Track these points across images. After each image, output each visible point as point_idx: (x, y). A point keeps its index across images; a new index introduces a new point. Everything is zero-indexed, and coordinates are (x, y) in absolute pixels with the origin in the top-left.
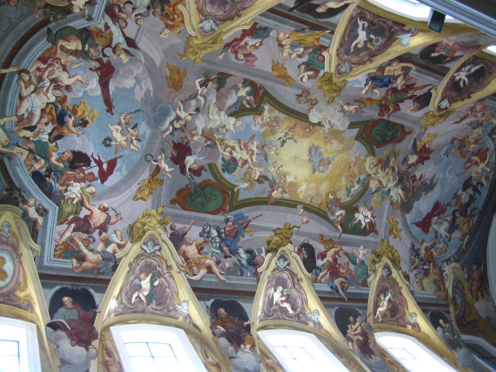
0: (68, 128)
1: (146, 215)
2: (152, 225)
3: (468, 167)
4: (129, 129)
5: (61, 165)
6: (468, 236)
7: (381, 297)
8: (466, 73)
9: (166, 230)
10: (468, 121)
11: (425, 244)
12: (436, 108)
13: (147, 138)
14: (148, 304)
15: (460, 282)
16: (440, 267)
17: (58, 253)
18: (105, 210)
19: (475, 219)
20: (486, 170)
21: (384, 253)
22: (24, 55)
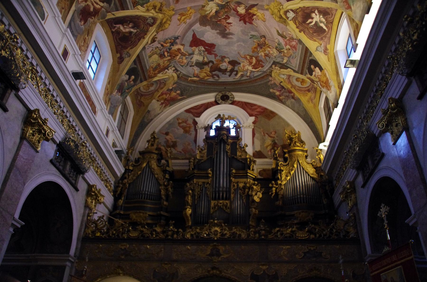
3: (246, 58)
6: (198, 79)
7: (131, 24)
8: (318, 20)
10: (281, 40)
11: (181, 47)
12: (286, 10)
15: (165, 85)
16: (170, 65)
19: (211, 80)
20: (248, 73)
21: (164, 14)
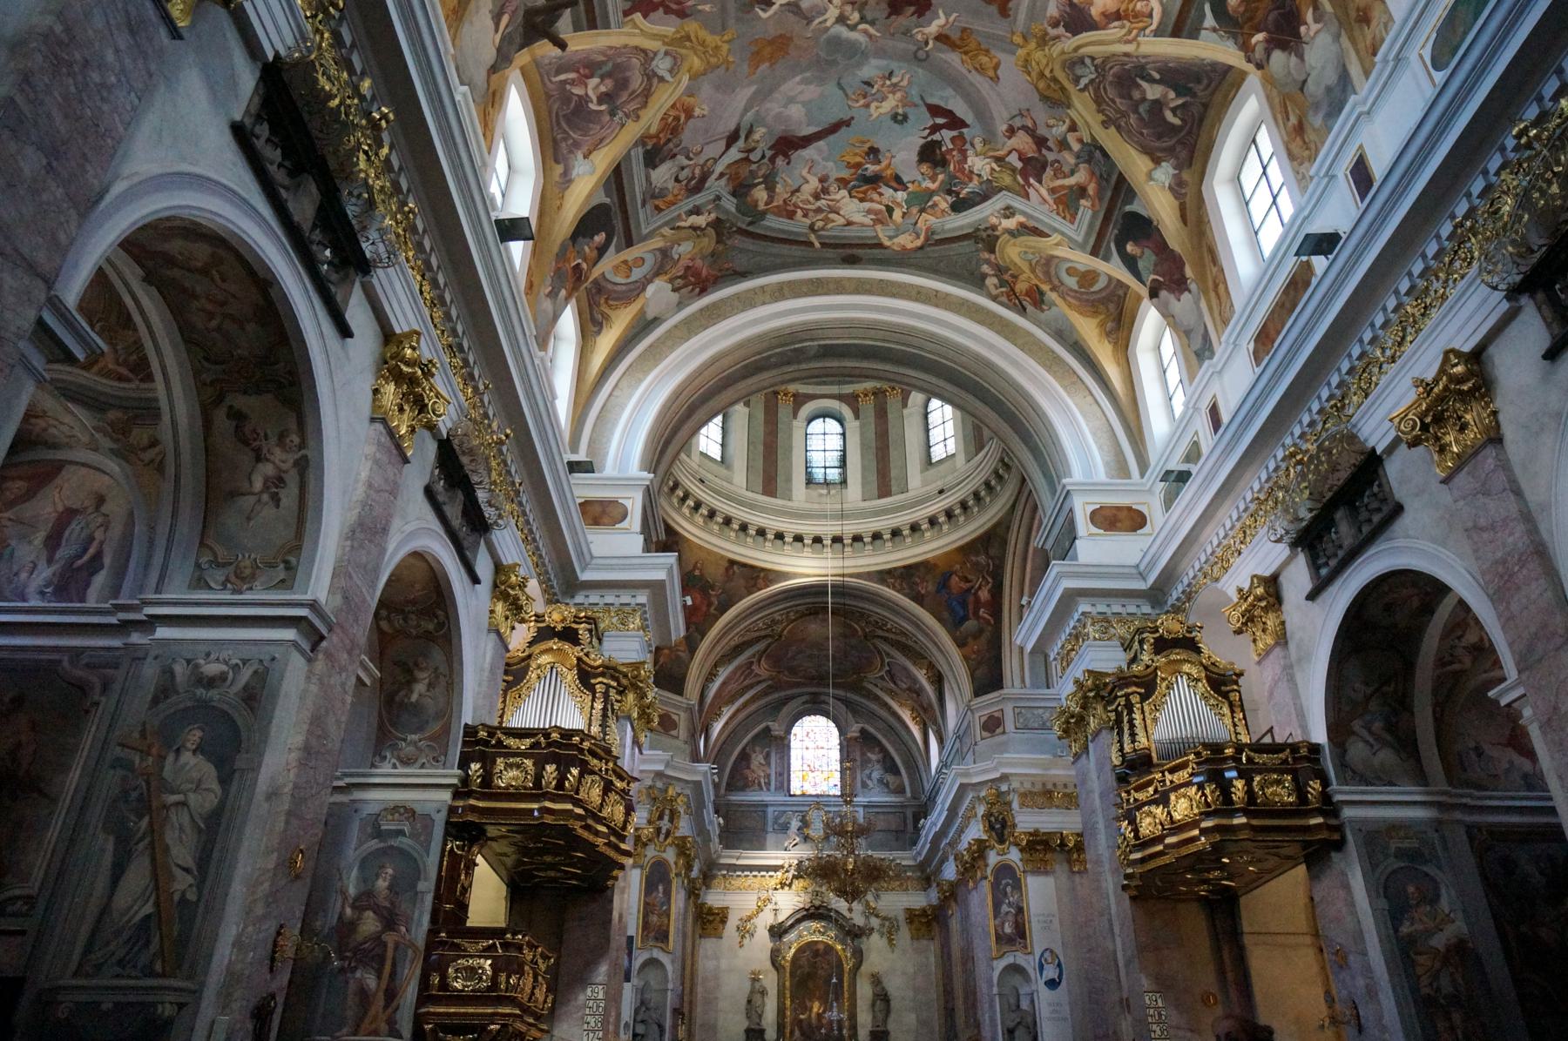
0: (882, 170)
1: (1026, 67)
2: (1044, 61)
4: (874, 91)
5: (941, 177)
9: (1057, 38)
13: (883, 63)
14: (1194, 95)
17: (1068, 217)
18: (1011, 131)
22: (792, 232)
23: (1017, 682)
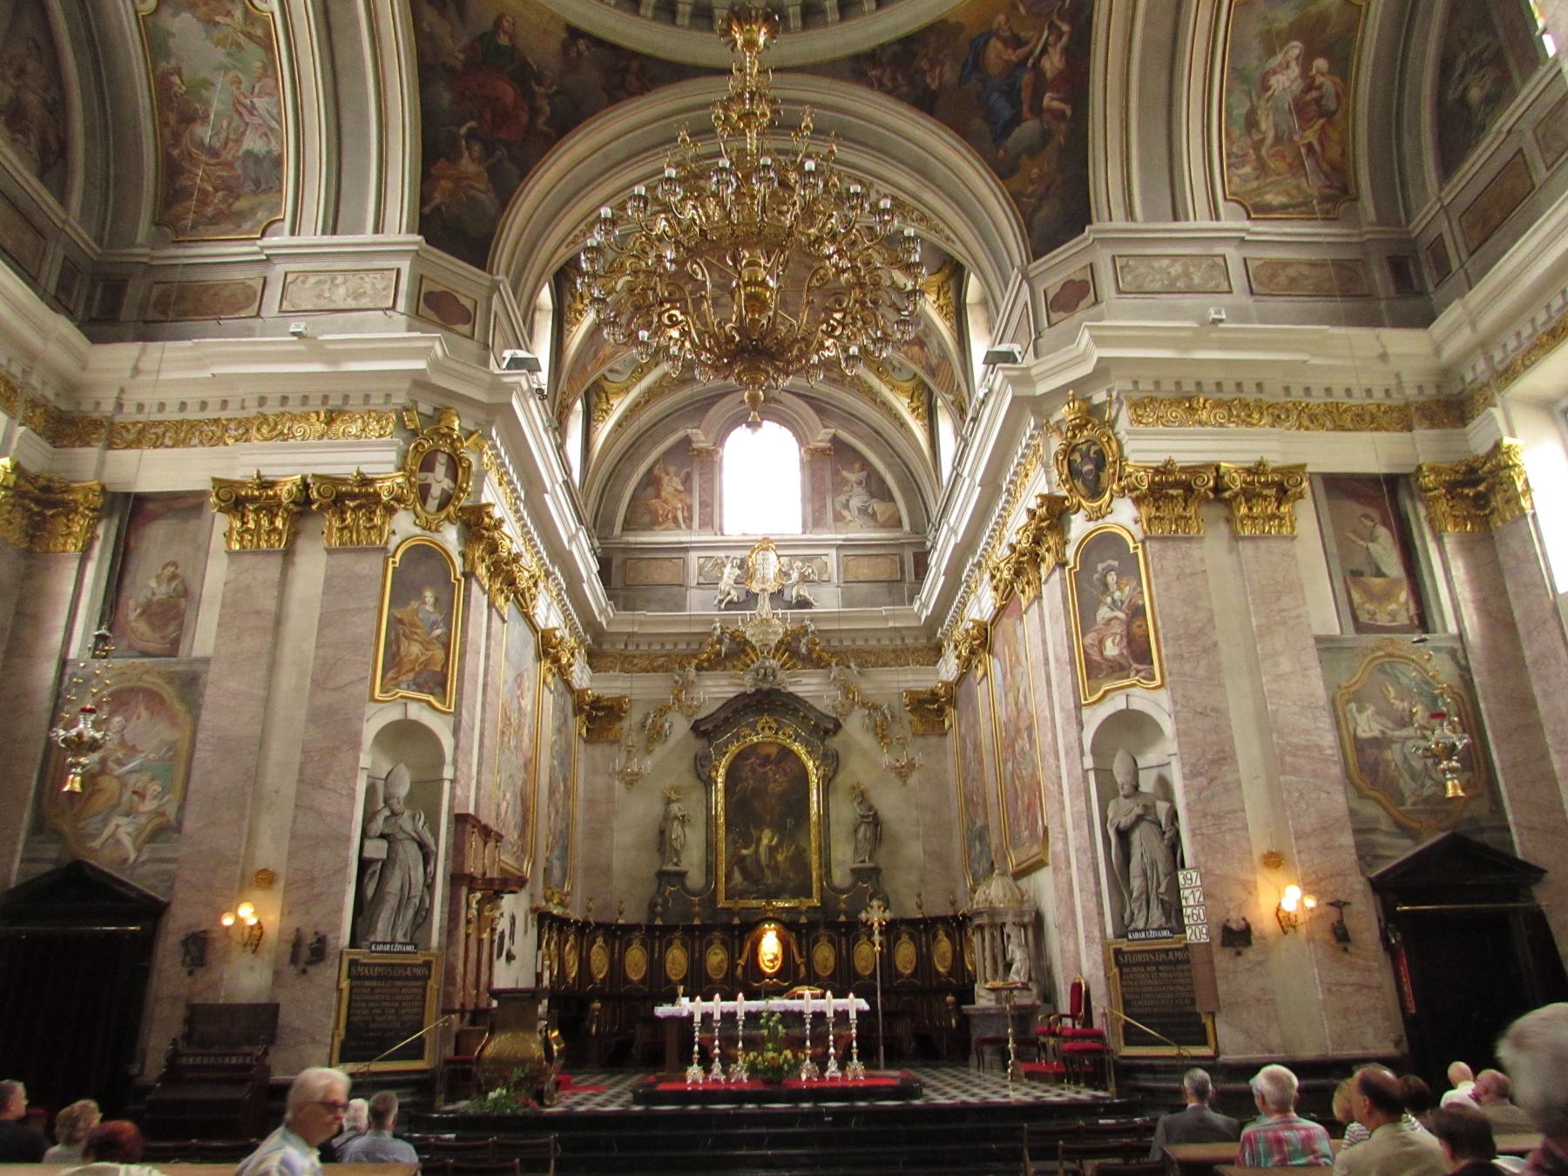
23: (1118, 211)
